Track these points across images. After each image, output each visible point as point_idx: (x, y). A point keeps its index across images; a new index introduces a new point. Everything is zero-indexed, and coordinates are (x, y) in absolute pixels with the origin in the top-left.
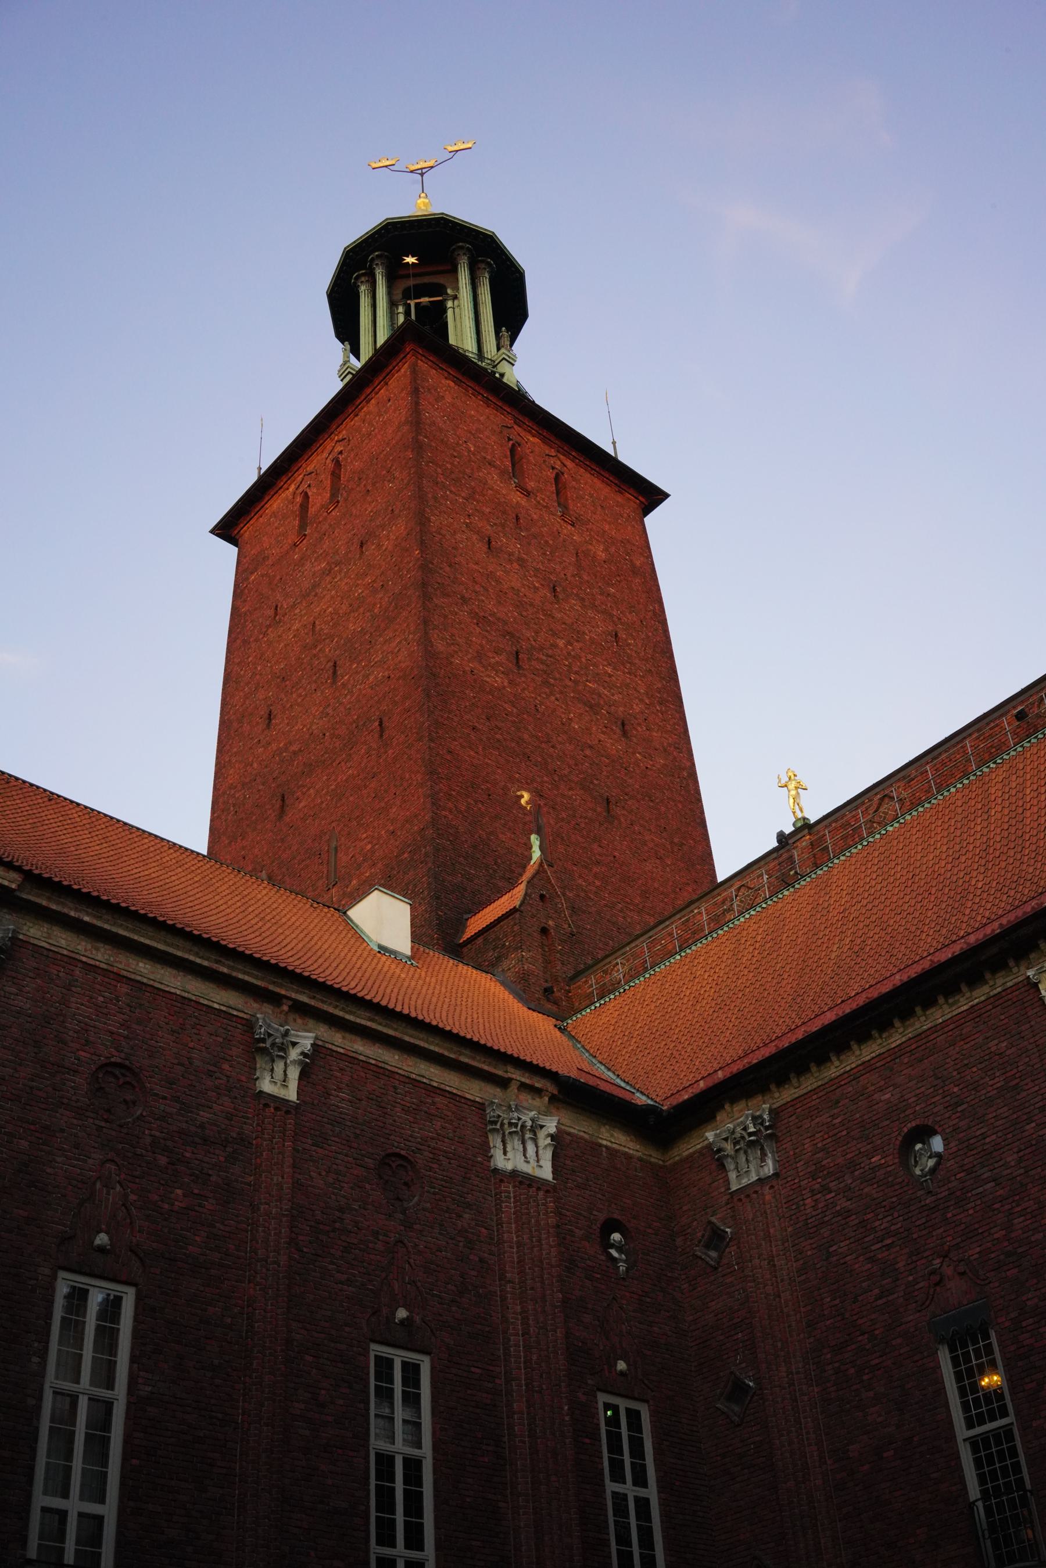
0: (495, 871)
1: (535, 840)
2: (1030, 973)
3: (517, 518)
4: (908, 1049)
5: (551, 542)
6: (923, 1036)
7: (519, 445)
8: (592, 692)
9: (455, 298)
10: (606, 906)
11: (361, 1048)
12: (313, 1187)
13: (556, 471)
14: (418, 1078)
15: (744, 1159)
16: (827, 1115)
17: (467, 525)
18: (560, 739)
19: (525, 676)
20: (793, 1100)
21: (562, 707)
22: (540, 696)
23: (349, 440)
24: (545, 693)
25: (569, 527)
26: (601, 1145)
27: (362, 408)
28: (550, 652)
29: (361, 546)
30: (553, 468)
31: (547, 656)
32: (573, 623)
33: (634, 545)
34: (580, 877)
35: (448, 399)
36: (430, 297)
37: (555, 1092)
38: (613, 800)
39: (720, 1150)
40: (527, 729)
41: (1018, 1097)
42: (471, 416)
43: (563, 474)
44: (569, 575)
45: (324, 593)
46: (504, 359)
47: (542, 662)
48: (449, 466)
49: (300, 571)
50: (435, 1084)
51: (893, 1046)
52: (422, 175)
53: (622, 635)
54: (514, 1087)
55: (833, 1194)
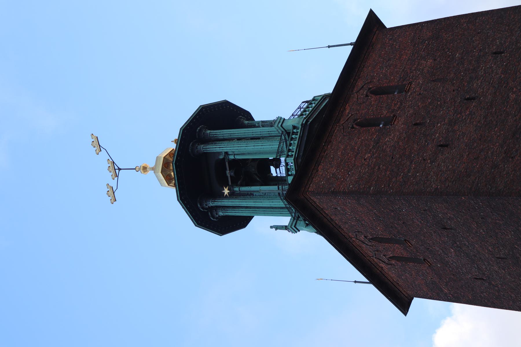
3: (416, 124)
5: (430, 101)
7: (355, 120)
9: (226, 153)
17: (431, 163)
23: (358, 232)
25: (413, 86)
27: (336, 223)
29: (445, 228)
30: (367, 96)
36: (226, 169)
43: (370, 89)
45: (475, 251)
46: (281, 126)
48: (388, 173)
49: (452, 264)
52: (120, 169)
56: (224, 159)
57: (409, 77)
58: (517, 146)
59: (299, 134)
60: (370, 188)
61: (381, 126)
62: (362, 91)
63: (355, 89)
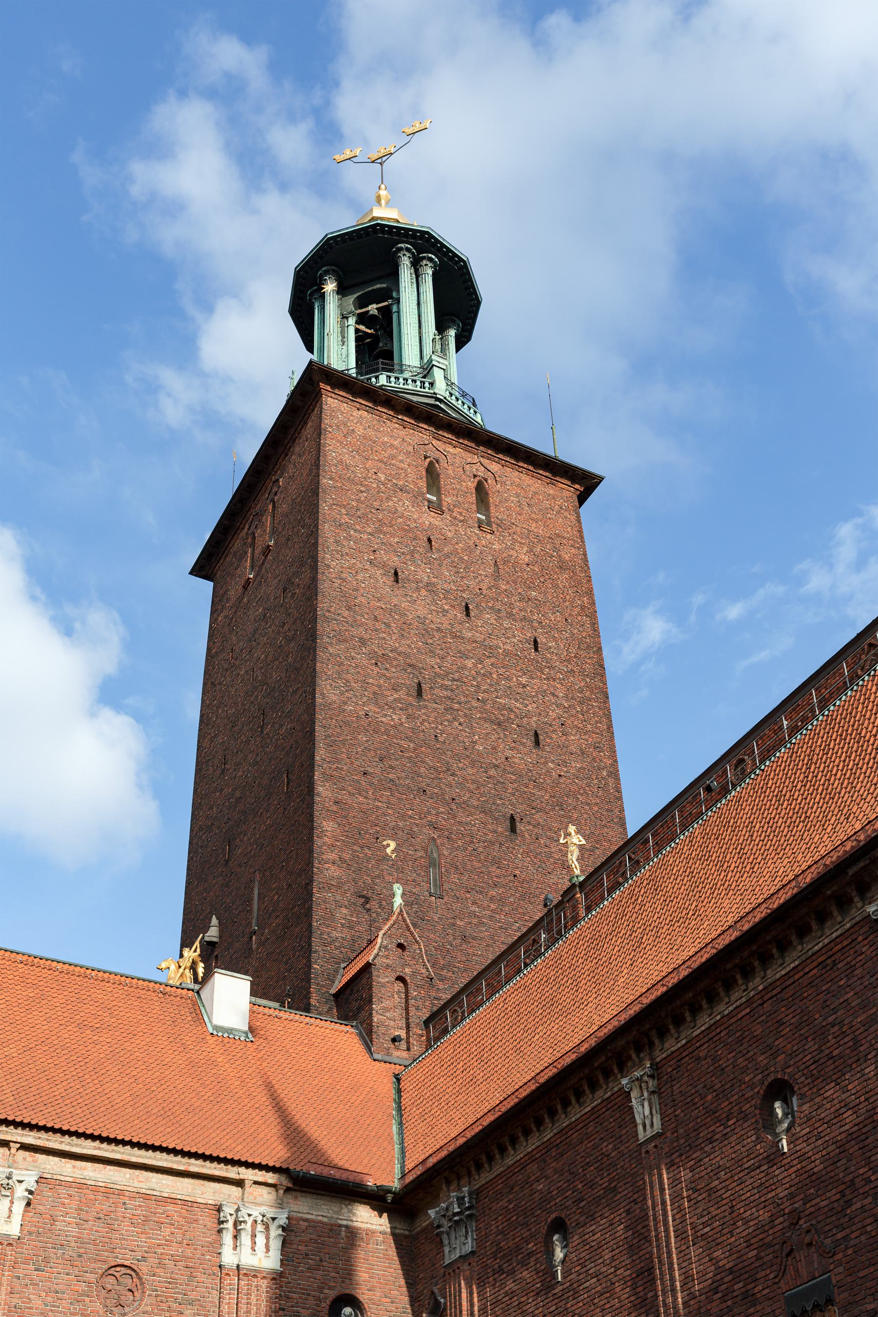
0: (378, 914)
1: (398, 889)
2: (624, 1081)
3: (429, 540)
4: (555, 1143)
5: (466, 558)
6: (564, 1132)
7: (437, 461)
8: (504, 707)
10: (501, 928)
11: (91, 1174)
12: (31, 1308)
13: (477, 479)
14: (148, 1192)
15: (454, 1236)
16: (506, 1200)
18: (461, 765)
19: (426, 707)
20: (487, 1183)
21: (466, 732)
22: (441, 724)
24: (448, 720)
25: (489, 536)
26: (340, 1226)
28: (456, 676)
30: (475, 476)
31: (454, 680)
32: (485, 640)
33: (564, 538)
34: (474, 903)
35: (360, 431)
37: (290, 1185)
38: (518, 819)
39: (439, 1226)
40: (423, 762)
41: (615, 1199)
42: (383, 443)
43: (486, 480)
44: (484, 588)
47: (444, 687)
48: (354, 504)
50: (166, 1195)
51: (545, 1139)
53: (541, 640)
54: (248, 1184)
55: (504, 1275)
56: (392, 298)
57: (503, 532)
58: (394, 670)
59: (422, 390)
60: (331, 479)
61: (428, 496)
62: (483, 469)
63: (485, 462)
